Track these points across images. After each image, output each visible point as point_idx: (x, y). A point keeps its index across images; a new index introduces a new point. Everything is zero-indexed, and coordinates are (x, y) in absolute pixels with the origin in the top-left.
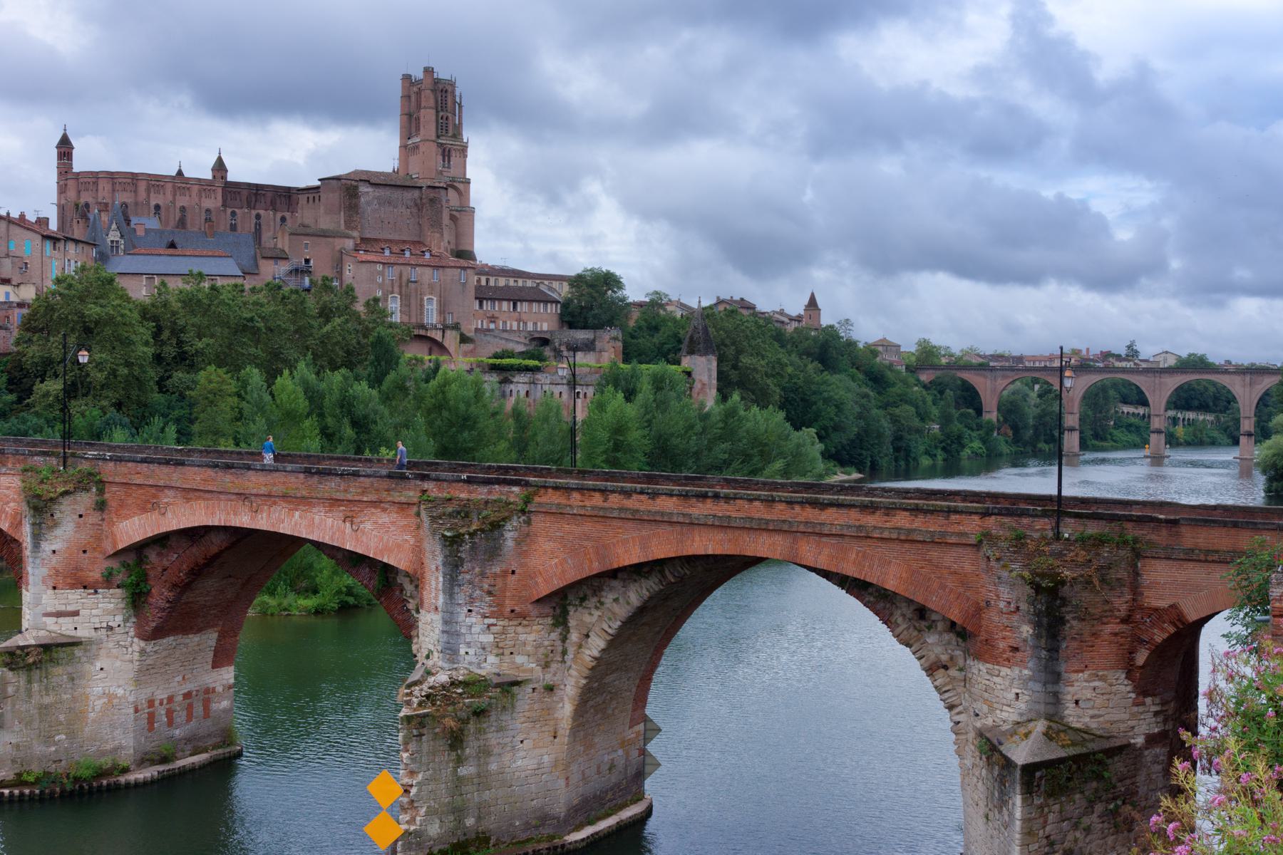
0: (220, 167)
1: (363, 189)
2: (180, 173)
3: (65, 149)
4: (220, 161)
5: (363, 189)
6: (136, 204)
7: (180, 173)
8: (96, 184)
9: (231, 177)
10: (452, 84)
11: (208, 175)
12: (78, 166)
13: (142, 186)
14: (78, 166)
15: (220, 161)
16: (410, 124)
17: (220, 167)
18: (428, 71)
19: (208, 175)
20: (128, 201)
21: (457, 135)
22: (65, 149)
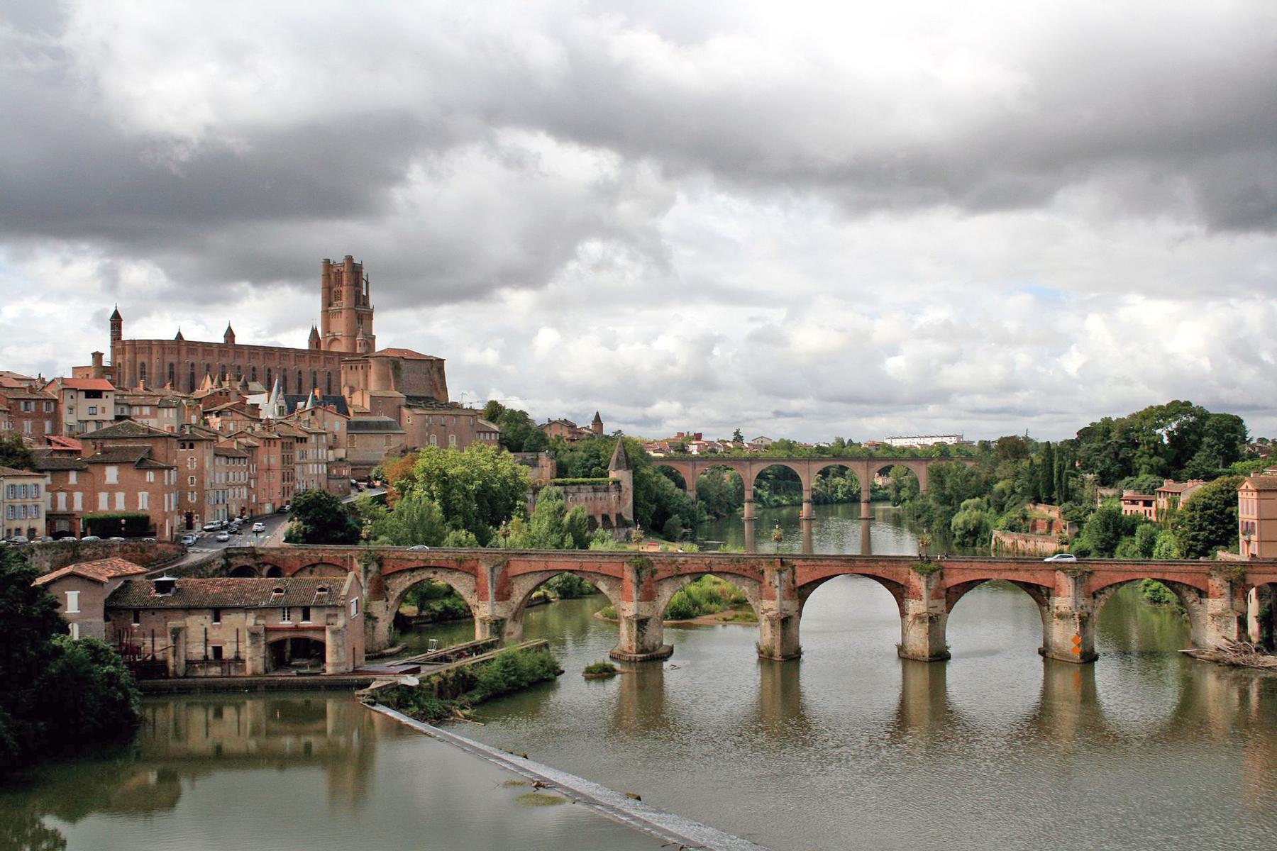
0: (230, 334)
1: (402, 362)
2: (179, 336)
3: (116, 321)
4: (230, 328)
5: (402, 362)
6: (179, 363)
7: (179, 336)
8: (150, 349)
9: (237, 342)
10: (360, 266)
11: (222, 340)
12: (127, 334)
13: (184, 351)
14: (127, 334)
15: (230, 328)
16: (330, 299)
17: (230, 334)
18: (349, 259)
19: (222, 340)
20: (175, 361)
21: (366, 304)
22: (116, 321)
